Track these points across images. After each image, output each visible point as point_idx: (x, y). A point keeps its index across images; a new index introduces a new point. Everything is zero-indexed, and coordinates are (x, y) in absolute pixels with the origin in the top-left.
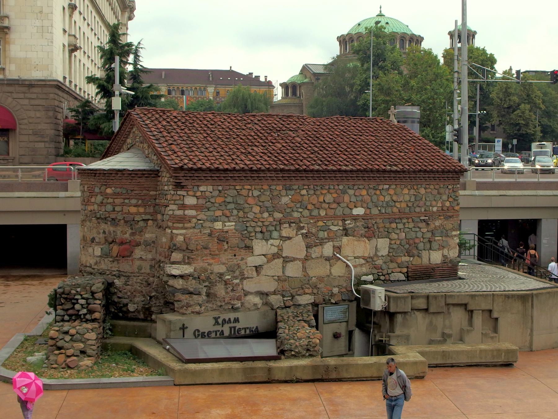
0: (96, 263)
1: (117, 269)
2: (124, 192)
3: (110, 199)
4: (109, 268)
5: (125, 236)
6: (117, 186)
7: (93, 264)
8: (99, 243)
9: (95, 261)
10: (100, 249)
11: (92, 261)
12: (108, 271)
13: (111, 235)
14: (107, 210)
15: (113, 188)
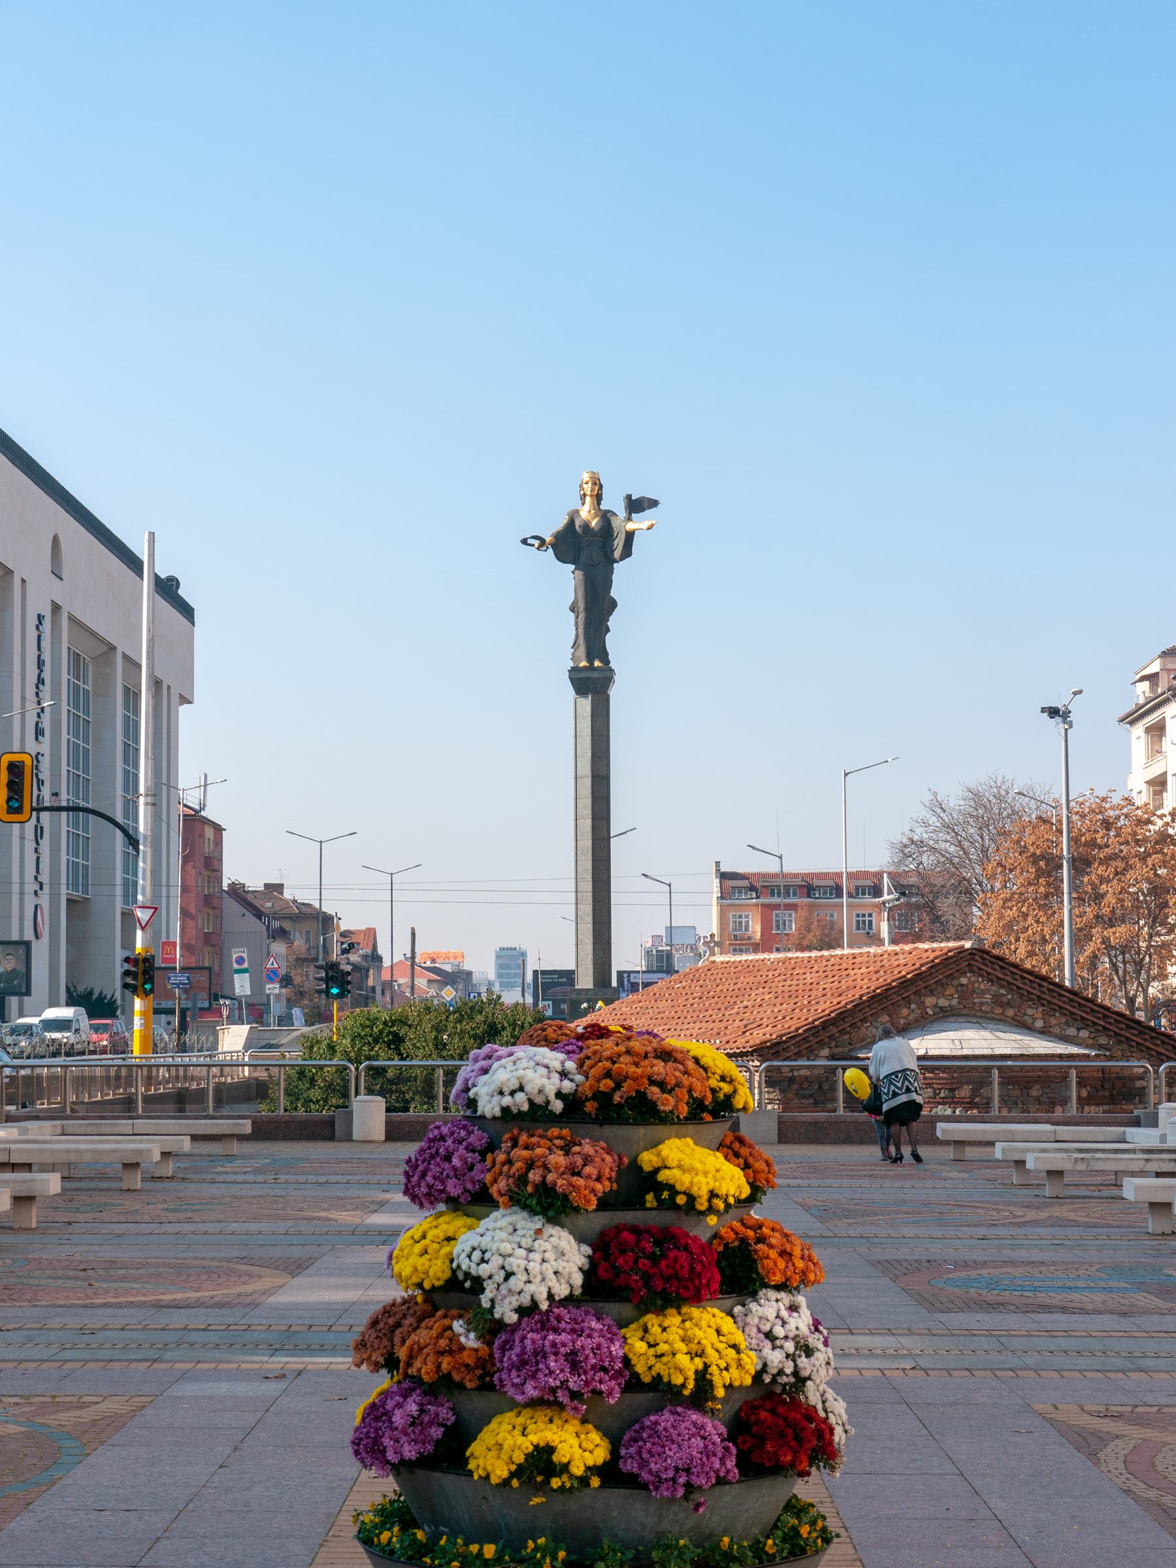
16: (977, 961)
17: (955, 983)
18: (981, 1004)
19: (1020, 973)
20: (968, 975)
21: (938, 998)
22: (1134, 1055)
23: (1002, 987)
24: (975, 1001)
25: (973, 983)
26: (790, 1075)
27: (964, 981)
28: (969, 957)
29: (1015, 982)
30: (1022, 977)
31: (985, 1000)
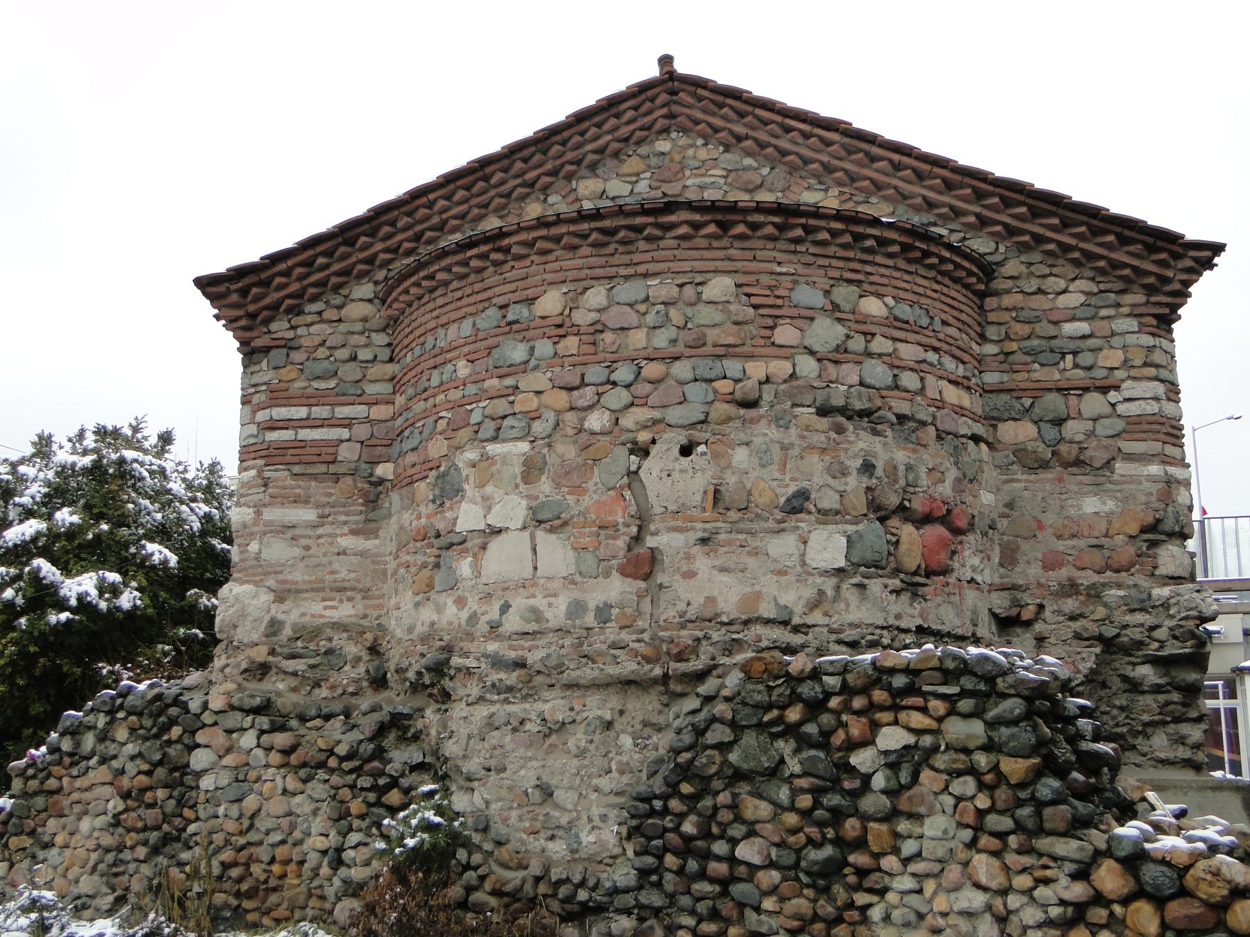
0: (816, 603)
1: (919, 622)
2: (925, 321)
3: (879, 338)
4: (892, 621)
5: (940, 488)
6: (902, 294)
7: (799, 609)
8: (826, 515)
9: (809, 593)
10: (844, 540)
11: (794, 597)
12: (885, 632)
13: (896, 481)
14: (868, 381)
15: (890, 302)
16: (690, 107)
17: (644, 150)
18: (702, 188)
19: (778, 118)
20: (674, 135)
21: (606, 180)
22: (1055, 270)
23: (749, 154)
24: (689, 182)
25: (684, 148)
26: (290, 334)
27: (663, 145)
28: (664, 97)
29: (774, 141)
30: (788, 130)
31: (708, 180)
